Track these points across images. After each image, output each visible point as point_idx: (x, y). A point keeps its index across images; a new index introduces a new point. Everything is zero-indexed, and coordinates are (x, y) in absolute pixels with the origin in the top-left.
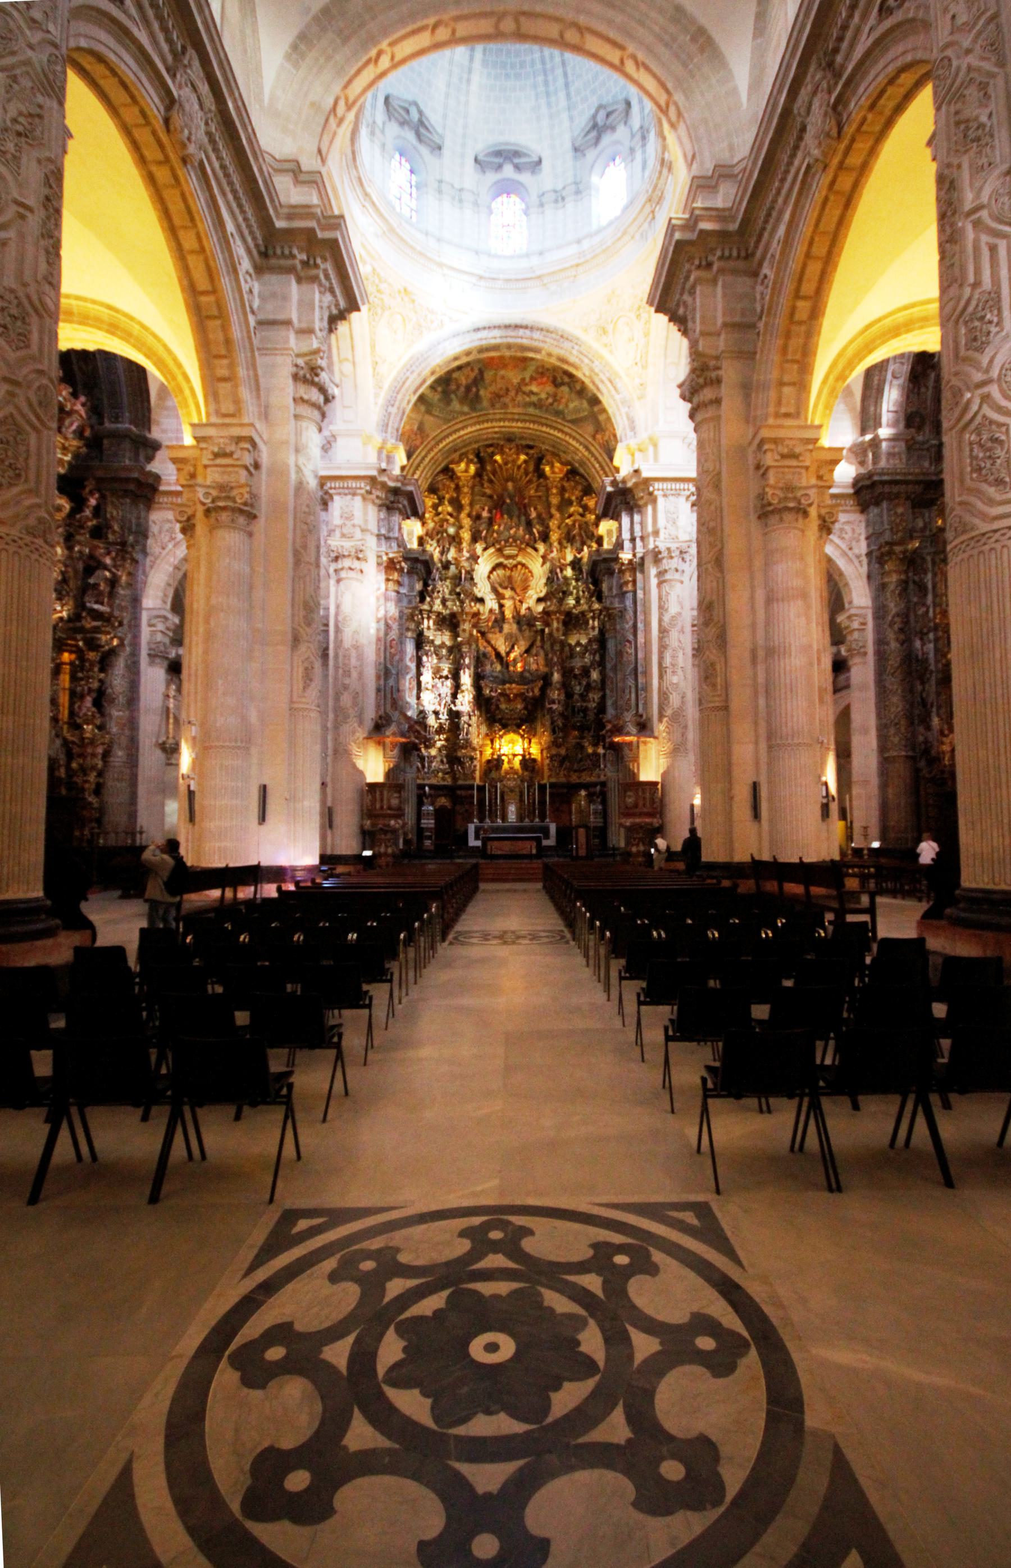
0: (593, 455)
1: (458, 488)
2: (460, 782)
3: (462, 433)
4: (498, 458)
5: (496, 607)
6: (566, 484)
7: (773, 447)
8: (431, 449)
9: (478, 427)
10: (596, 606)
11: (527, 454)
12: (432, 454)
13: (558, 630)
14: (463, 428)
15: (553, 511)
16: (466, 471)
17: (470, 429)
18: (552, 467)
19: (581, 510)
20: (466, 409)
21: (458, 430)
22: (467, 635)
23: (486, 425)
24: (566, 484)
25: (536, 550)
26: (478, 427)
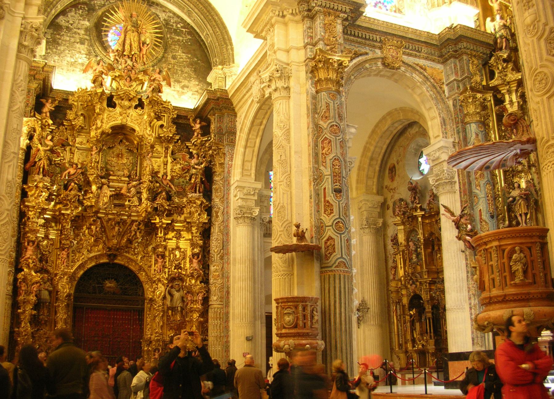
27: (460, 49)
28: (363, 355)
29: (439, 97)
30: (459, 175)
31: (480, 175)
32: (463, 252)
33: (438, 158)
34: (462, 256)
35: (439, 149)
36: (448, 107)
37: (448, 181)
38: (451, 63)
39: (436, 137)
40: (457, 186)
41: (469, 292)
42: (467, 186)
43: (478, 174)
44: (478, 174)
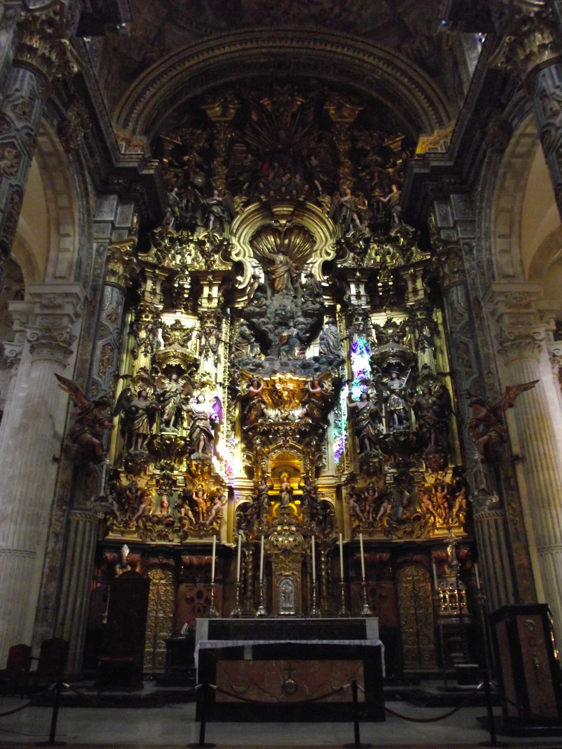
0: (399, 69)
1: (211, 138)
2: (190, 540)
3: (217, 52)
4: (266, 102)
5: (260, 272)
6: (356, 133)
7: (502, 298)
8: (174, 66)
9: (239, 47)
10: (418, 256)
11: (305, 98)
12: (175, 72)
13: (358, 296)
14: (218, 47)
15: (343, 159)
16: (223, 115)
17: (227, 49)
18: (339, 110)
19: (379, 159)
20: (223, 24)
21: (212, 49)
22: (215, 303)
23: (249, 45)
24: (356, 133)
25: (319, 204)
26: (239, 47)
27: (136, 190)
28: (491, 609)
29: (86, 229)
30: (79, 345)
31: (108, 359)
32: (55, 460)
33: (60, 307)
34: (53, 468)
35: (67, 295)
36: (91, 248)
37: (64, 345)
38: (114, 199)
39: (56, 278)
40: (72, 360)
41: (49, 528)
42: (87, 366)
43: (107, 357)
44: (107, 357)
